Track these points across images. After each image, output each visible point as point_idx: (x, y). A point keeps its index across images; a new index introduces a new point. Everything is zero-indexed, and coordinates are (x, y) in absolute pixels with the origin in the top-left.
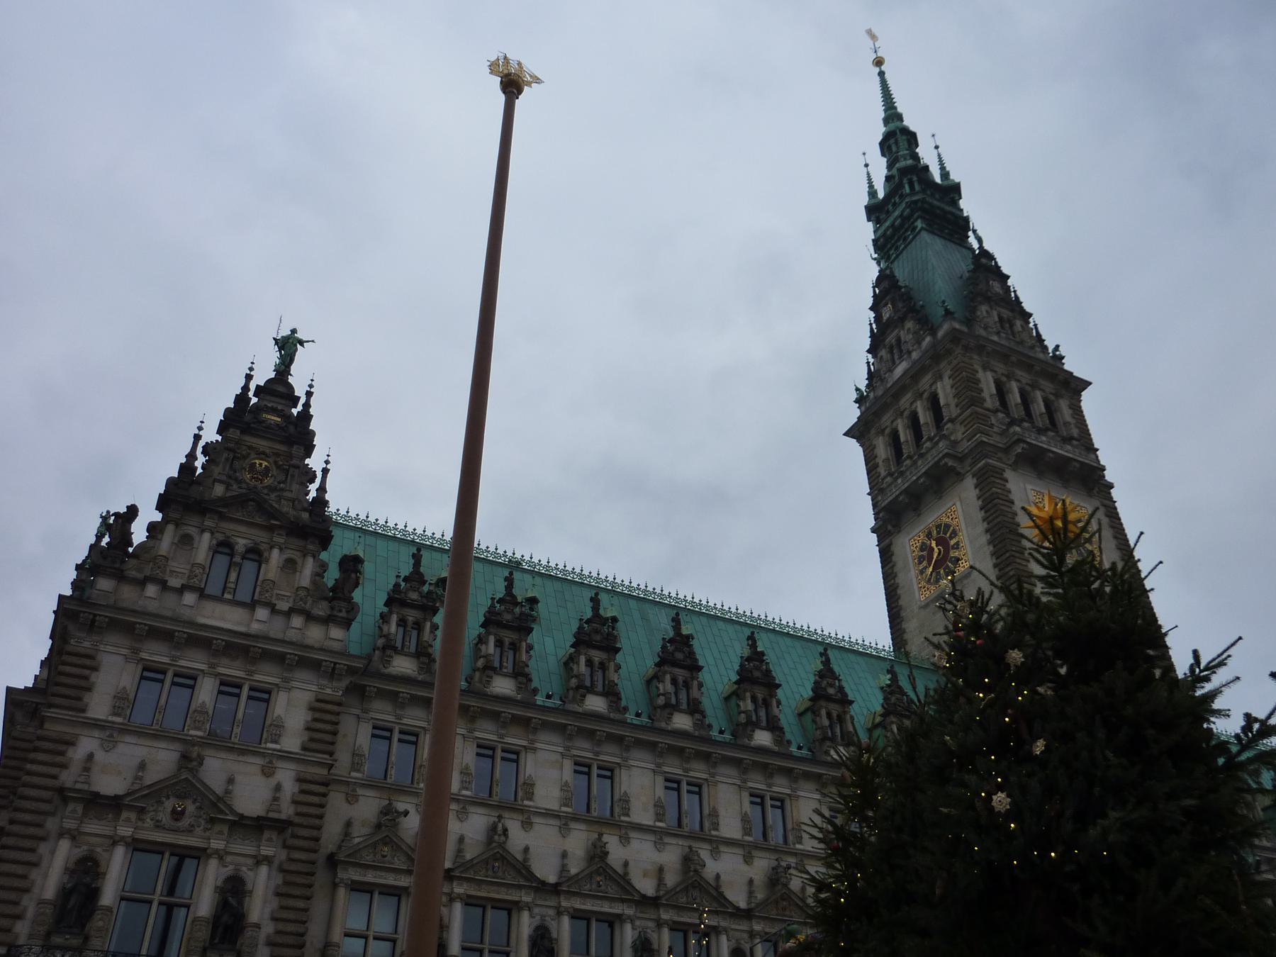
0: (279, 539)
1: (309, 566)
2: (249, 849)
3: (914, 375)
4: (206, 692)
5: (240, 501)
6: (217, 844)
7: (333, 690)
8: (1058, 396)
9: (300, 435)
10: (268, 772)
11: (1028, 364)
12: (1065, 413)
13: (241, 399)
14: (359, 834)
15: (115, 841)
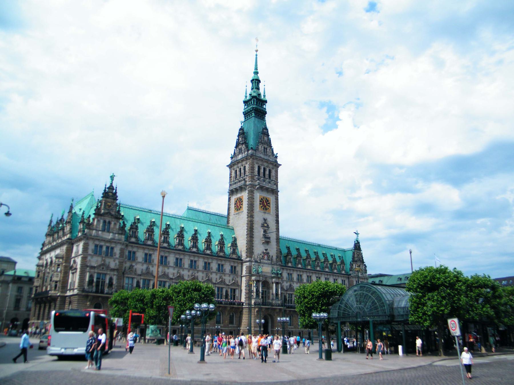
0: (113, 220)
1: (118, 224)
2: (112, 273)
3: (242, 160)
4: (104, 249)
5: (107, 213)
6: (108, 273)
7: (123, 247)
8: (273, 169)
9: (114, 196)
10: (114, 261)
11: (267, 161)
12: (273, 173)
13: (105, 190)
14: (127, 268)
15: (95, 272)
